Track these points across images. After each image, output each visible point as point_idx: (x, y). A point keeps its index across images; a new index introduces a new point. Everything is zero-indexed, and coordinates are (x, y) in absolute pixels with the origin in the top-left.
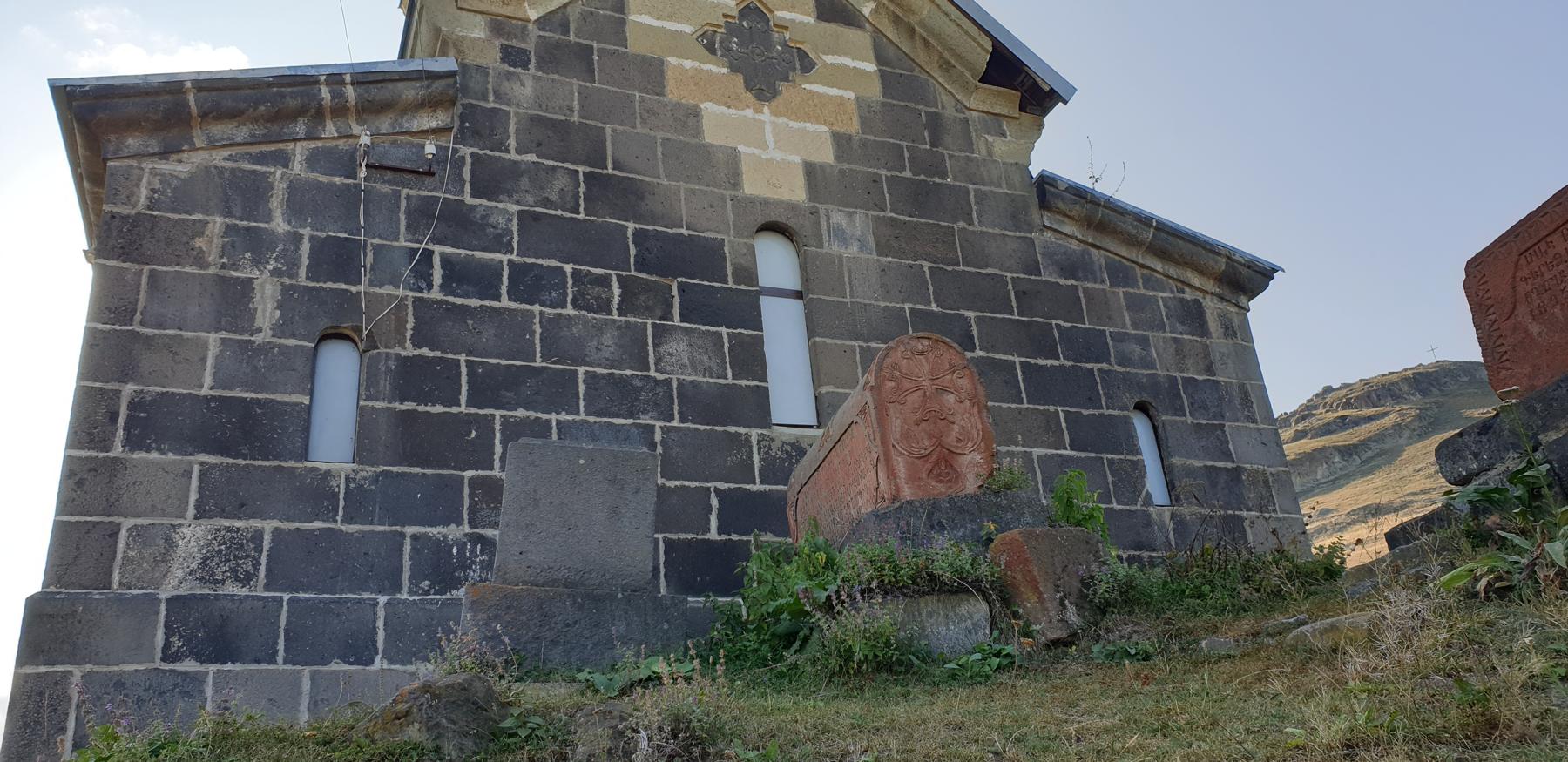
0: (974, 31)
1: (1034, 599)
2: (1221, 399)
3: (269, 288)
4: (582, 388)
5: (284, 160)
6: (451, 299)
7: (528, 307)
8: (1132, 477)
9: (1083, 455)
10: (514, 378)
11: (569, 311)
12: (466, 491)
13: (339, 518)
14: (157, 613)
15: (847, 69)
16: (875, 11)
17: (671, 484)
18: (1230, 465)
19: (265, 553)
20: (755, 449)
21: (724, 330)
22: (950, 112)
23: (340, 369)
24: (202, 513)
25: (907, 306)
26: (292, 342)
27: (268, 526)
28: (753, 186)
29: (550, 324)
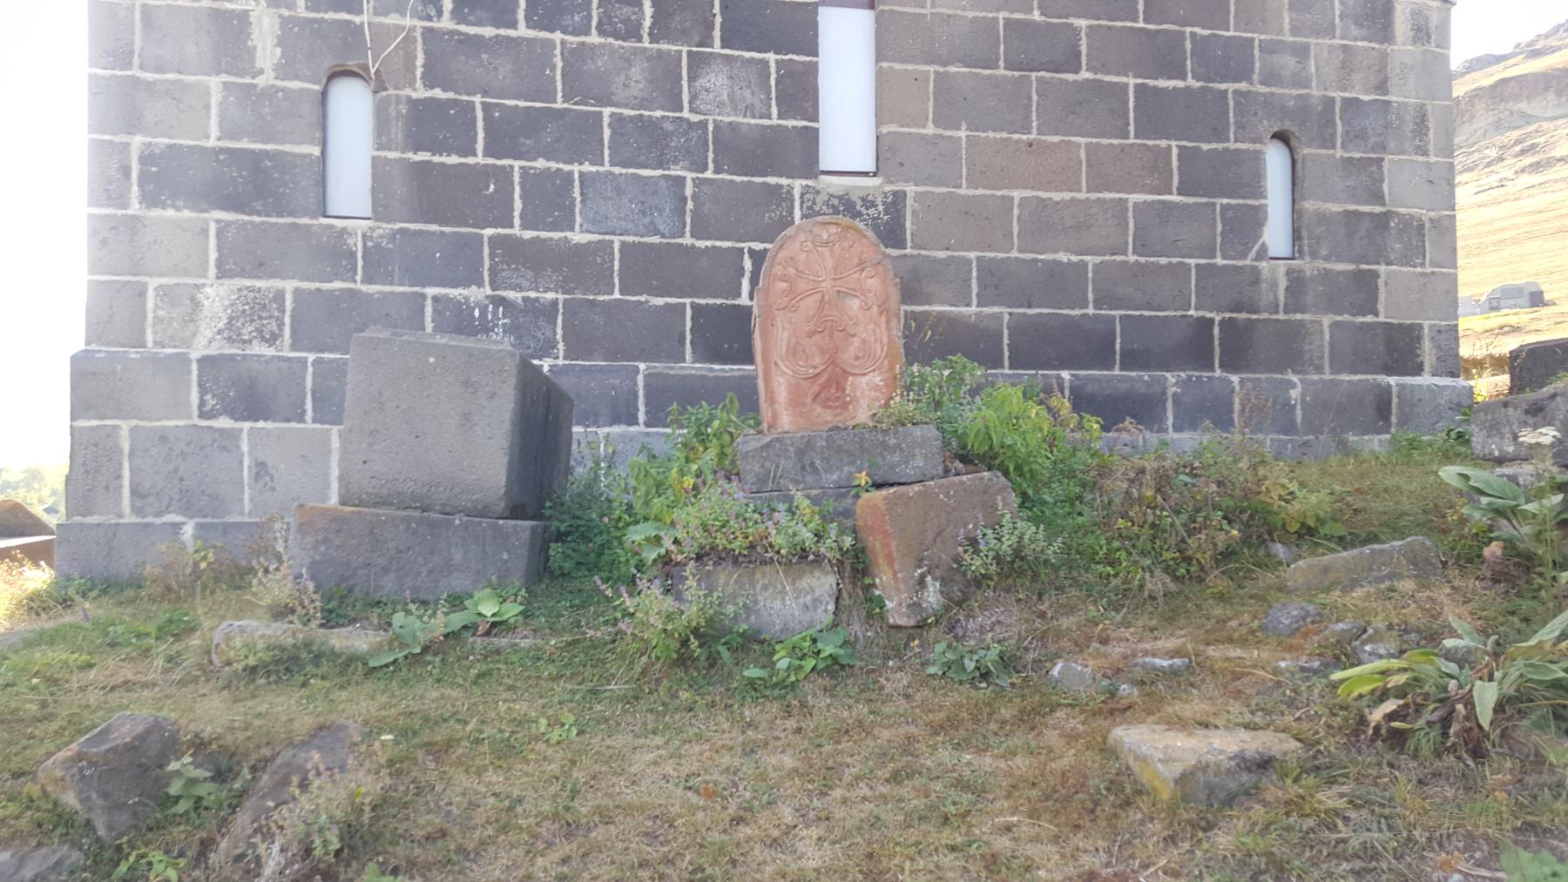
1: (890, 575)
2: (1387, 126)
3: (266, 20)
4: (607, 133)
6: (463, 28)
7: (547, 35)
8: (1247, 224)
9: (1191, 200)
10: (532, 122)
11: (594, 38)
12: (486, 251)
13: (358, 278)
14: (189, 372)
17: (702, 244)
18: (1378, 209)
19: (288, 314)
20: (797, 204)
21: (771, 57)
23: (352, 107)
24: (222, 273)
25: (1001, 15)
26: (296, 85)
27: (289, 286)
29: (575, 57)
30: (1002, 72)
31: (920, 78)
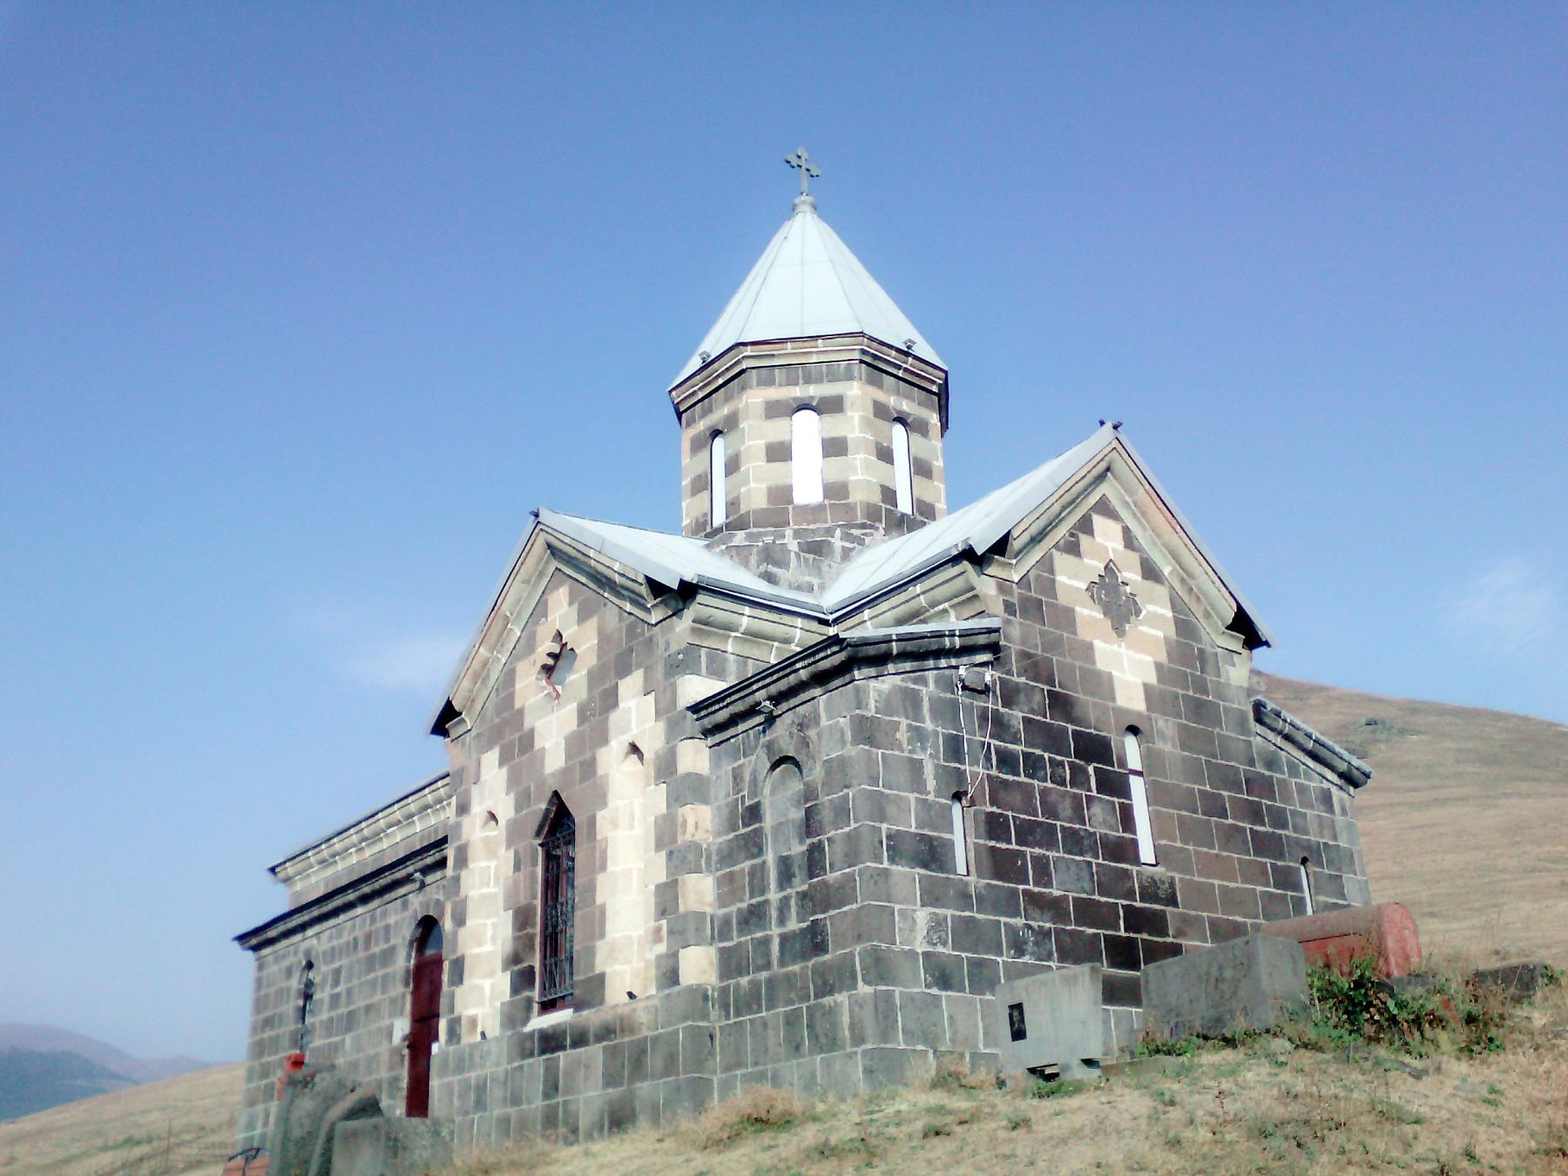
5: (926, 684)
11: (1049, 785)
15: (1156, 611)
17: (1103, 899)
22: (1209, 649)
27: (949, 912)
28: (1122, 701)
31: (1171, 816)
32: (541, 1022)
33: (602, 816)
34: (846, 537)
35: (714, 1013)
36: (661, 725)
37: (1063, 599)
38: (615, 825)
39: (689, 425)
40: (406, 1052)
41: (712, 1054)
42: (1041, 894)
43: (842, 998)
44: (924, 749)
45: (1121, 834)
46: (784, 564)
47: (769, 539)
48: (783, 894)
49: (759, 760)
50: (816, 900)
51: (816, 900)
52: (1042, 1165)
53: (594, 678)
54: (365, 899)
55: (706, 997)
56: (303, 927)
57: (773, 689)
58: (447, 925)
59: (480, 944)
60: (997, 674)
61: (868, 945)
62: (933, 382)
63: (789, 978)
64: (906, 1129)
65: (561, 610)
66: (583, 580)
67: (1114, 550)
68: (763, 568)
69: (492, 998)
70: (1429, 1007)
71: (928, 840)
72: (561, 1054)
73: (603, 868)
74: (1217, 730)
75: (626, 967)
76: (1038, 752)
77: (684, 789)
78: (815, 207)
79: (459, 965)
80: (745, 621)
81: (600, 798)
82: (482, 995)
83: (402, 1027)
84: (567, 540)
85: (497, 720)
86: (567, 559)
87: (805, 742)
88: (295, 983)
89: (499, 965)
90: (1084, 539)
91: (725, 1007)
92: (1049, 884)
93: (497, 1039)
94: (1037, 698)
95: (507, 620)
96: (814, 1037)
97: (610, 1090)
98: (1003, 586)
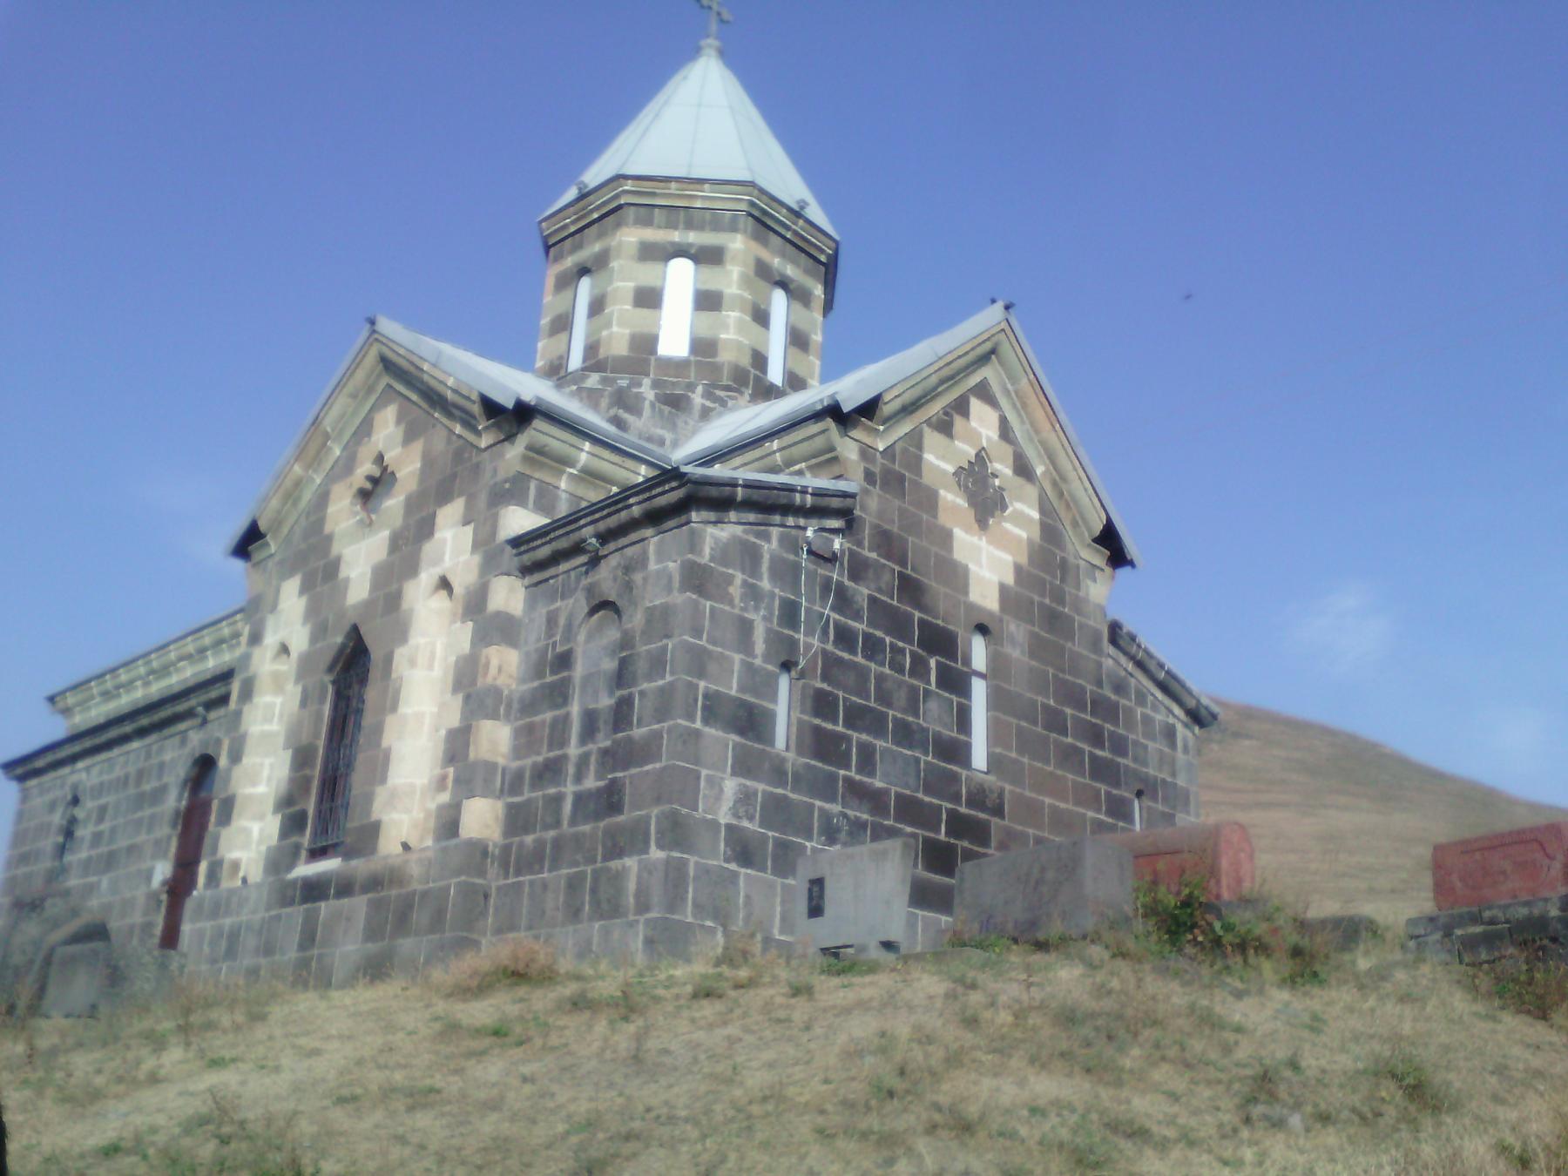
0: (1098, 504)
5: (768, 540)
15: (1024, 510)
16: (1044, 474)
17: (927, 799)
22: (1071, 559)
27: (761, 787)
28: (975, 596)
30: (1039, 729)
32: (306, 870)
33: (401, 654)
34: (708, 395)
35: (493, 870)
36: (477, 559)
37: (927, 479)
38: (413, 663)
39: (556, 260)
40: (164, 897)
41: (484, 913)
42: (861, 783)
43: (631, 863)
44: (757, 609)
45: (954, 734)
46: (636, 410)
47: (623, 383)
48: (585, 749)
49: (578, 604)
50: (616, 757)
51: (616, 757)
52: (818, 1031)
53: (412, 505)
54: (142, 733)
55: (485, 853)
56: (74, 759)
57: (602, 526)
58: (223, 762)
59: (254, 784)
60: (847, 545)
61: (666, 807)
62: (822, 251)
63: (578, 839)
64: (675, 990)
65: (387, 430)
66: (414, 397)
67: (989, 439)
68: (613, 412)
69: (260, 842)
70: (1257, 931)
71: (750, 709)
72: (323, 904)
73: (394, 708)
74: (1069, 645)
75: (405, 817)
76: (879, 634)
77: (492, 629)
78: (722, 53)
79: (228, 805)
80: (583, 457)
81: (401, 633)
82: (249, 839)
83: (162, 870)
84: (402, 351)
85: (303, 546)
86: (399, 372)
87: (629, 586)
88: (57, 819)
89: (270, 805)
90: (958, 421)
91: (505, 865)
92: (872, 774)
93: (258, 886)
94: (887, 577)
95: (327, 437)
96: (596, 903)
97: (370, 945)
98: (866, 452)
